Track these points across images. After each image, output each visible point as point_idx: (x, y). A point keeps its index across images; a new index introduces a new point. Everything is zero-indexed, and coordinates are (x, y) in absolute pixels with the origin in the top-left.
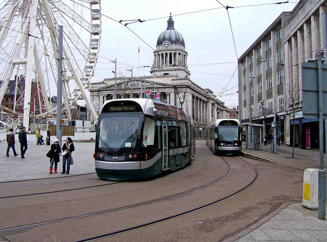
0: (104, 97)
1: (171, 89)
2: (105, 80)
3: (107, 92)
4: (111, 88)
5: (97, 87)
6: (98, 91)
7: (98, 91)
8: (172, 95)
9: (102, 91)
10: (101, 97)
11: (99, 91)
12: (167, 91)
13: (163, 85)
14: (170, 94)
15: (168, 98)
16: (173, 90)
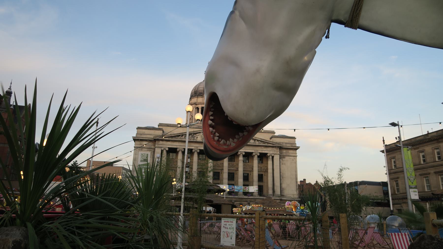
0: (162, 151)
1: (275, 149)
2: (160, 125)
3: (169, 143)
4: (179, 139)
5: (151, 134)
6: (150, 141)
7: (150, 141)
8: (277, 158)
9: (161, 142)
10: (158, 151)
11: (155, 140)
12: (269, 151)
13: (264, 142)
14: (273, 157)
15: (270, 162)
16: (277, 151)
